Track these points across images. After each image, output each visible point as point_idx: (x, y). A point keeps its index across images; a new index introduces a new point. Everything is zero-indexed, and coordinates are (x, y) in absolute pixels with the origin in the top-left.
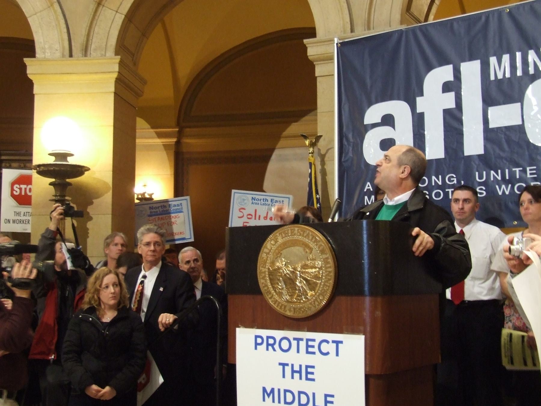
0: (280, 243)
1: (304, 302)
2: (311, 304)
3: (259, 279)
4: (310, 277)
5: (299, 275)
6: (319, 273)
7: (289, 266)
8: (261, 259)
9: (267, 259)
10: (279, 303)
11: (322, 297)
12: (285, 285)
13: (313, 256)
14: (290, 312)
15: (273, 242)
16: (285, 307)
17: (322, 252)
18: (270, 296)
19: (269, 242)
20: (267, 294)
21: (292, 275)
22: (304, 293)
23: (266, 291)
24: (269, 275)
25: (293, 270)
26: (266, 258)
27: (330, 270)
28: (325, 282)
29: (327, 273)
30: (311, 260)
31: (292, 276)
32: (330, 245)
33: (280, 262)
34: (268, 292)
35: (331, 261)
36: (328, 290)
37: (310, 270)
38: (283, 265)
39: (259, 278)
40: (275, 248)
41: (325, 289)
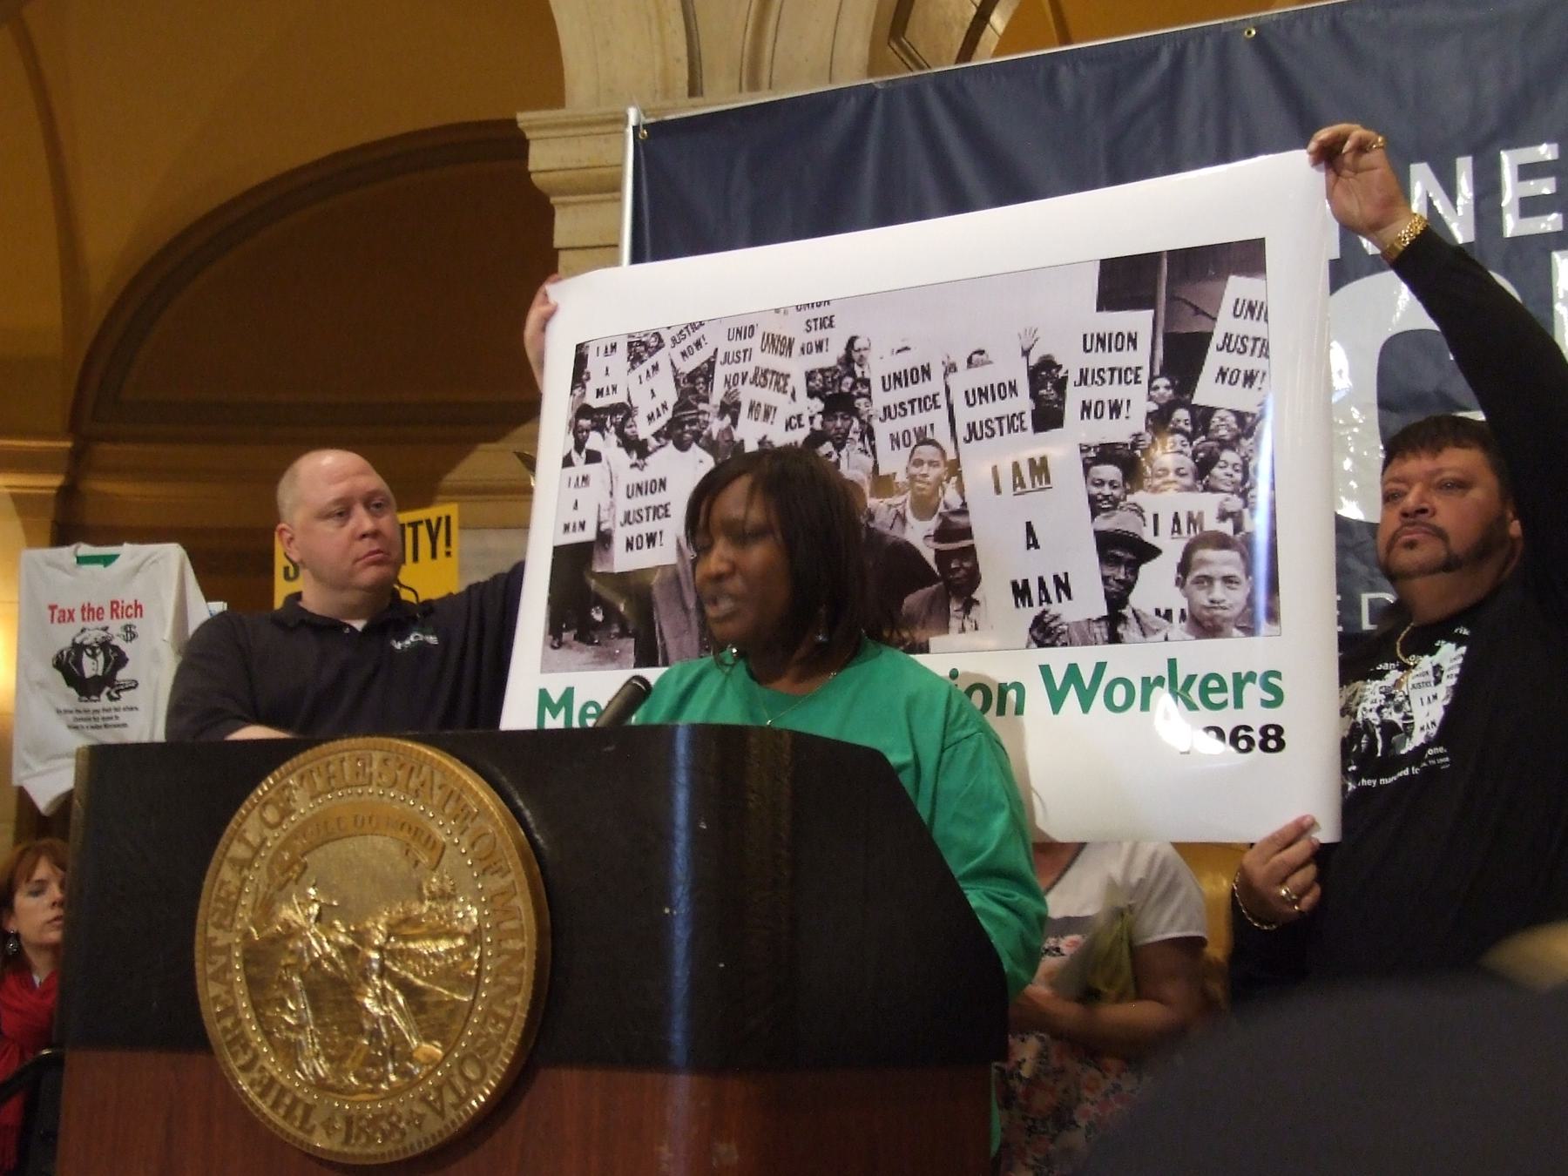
0: (303, 819)
1: (395, 1092)
2: (423, 1099)
3: (199, 982)
4: (424, 974)
5: (375, 966)
6: (467, 957)
7: (337, 923)
8: (217, 885)
9: (240, 891)
10: (283, 1091)
11: (478, 1072)
12: (312, 1009)
13: (442, 880)
14: (328, 1135)
15: (271, 815)
16: (309, 1109)
17: (488, 864)
18: (244, 1059)
19: (255, 813)
20: (229, 1050)
21: (347, 962)
22: (398, 1049)
23: (229, 1037)
24: (246, 963)
25: (350, 942)
26: (238, 883)
27: (513, 944)
28: (490, 1001)
29: (505, 958)
30: (433, 898)
31: (344, 967)
32: (523, 833)
33: (296, 902)
34: (235, 1039)
35: (522, 903)
36: (503, 1037)
37: (425, 946)
38: (308, 917)
39: (199, 973)
40: (278, 842)
41: (489, 1034)
